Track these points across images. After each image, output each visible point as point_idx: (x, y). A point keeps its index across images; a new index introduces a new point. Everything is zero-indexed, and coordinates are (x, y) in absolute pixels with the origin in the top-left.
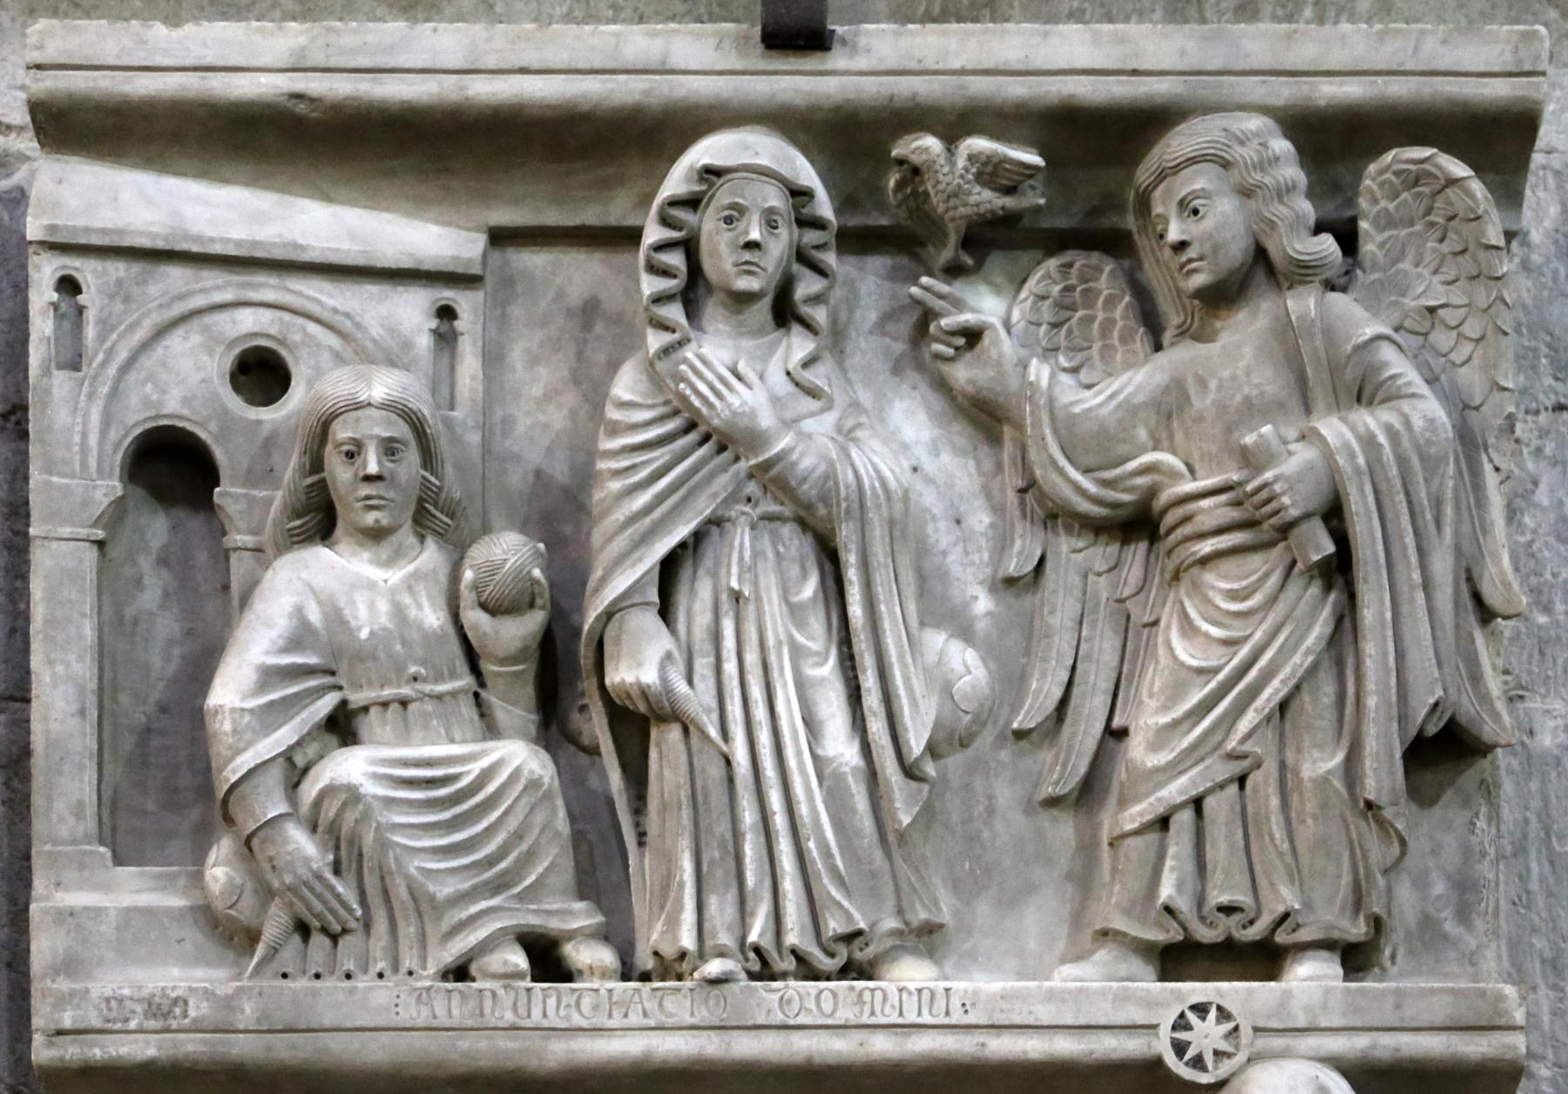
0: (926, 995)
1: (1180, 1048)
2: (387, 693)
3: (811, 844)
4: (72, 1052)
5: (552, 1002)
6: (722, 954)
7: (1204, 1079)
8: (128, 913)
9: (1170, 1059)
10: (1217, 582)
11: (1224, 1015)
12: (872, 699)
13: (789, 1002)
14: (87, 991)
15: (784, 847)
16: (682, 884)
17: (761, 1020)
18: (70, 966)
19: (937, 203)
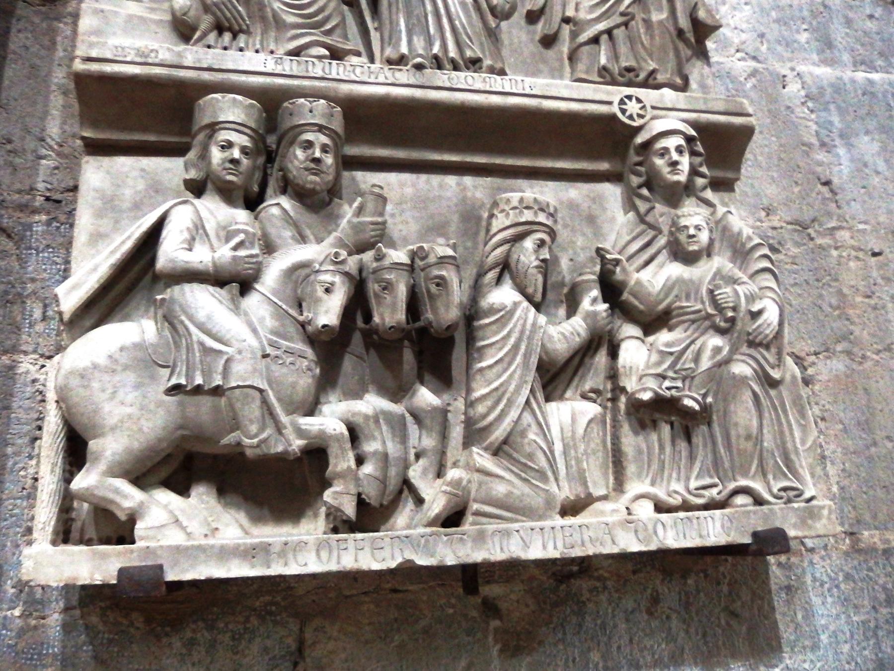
0: (513, 81)
1: (623, 111)
3: (457, 22)
9: (620, 115)
11: (639, 101)
15: (445, 21)
16: (400, 31)
17: (440, 84)
18: (97, 32)
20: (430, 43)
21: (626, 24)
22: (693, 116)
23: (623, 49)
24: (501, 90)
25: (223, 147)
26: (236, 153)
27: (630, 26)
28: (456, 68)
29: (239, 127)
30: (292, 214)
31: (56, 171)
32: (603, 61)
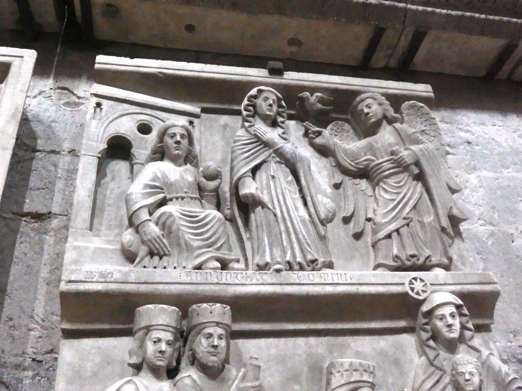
0: (339, 275)
1: (412, 289)
2: (178, 195)
3: (300, 236)
4: (73, 287)
5: (228, 276)
6: (278, 263)
7: (421, 298)
8: (96, 249)
9: (410, 292)
10: (391, 181)
11: (422, 280)
12: (310, 203)
13: (300, 277)
14: (81, 269)
16: (265, 245)
17: (292, 282)
18: (76, 262)
19: (308, 107)
20: (284, 252)
21: (408, 225)
22: (458, 288)
23: (407, 241)
24: (331, 282)
25: (155, 342)
26: (163, 346)
27: (410, 226)
28: (302, 268)
29: (165, 328)
30: (199, 382)
31: (40, 340)
32: (395, 251)
